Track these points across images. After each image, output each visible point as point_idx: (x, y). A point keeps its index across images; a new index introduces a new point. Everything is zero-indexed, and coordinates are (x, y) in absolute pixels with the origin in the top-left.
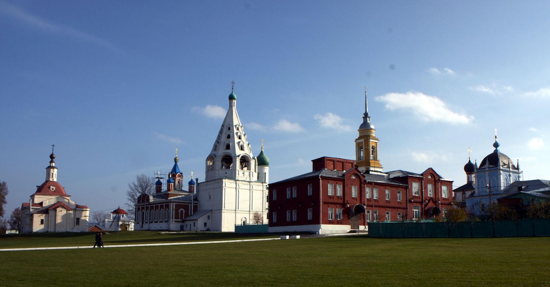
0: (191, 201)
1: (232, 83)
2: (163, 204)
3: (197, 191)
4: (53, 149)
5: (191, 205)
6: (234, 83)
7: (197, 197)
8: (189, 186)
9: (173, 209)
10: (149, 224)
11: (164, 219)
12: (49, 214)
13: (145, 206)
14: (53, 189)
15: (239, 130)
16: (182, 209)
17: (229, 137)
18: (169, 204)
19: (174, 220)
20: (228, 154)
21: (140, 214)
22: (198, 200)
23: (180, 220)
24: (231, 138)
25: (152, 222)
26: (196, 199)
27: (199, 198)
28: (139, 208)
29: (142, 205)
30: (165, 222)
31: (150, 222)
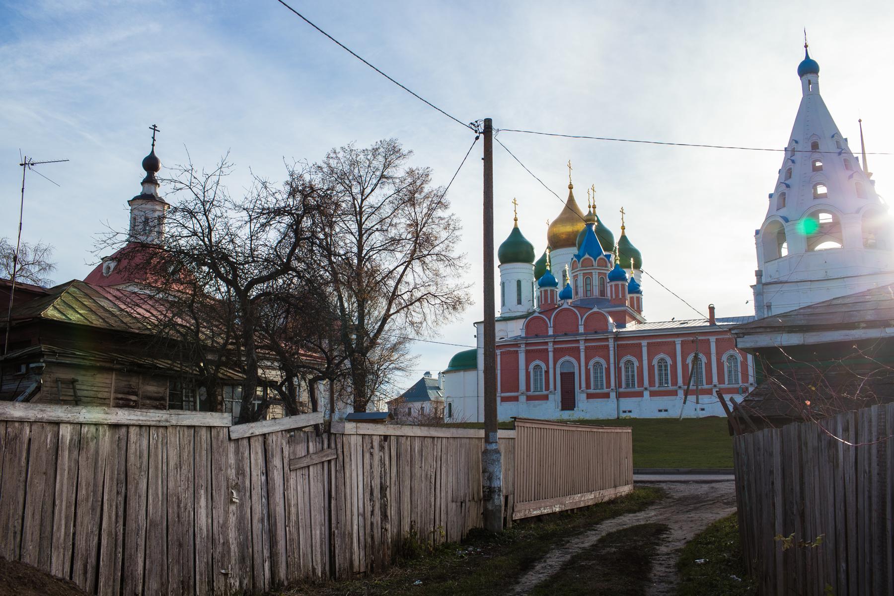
4: (154, 140)
11: (715, 380)
31: (619, 396)
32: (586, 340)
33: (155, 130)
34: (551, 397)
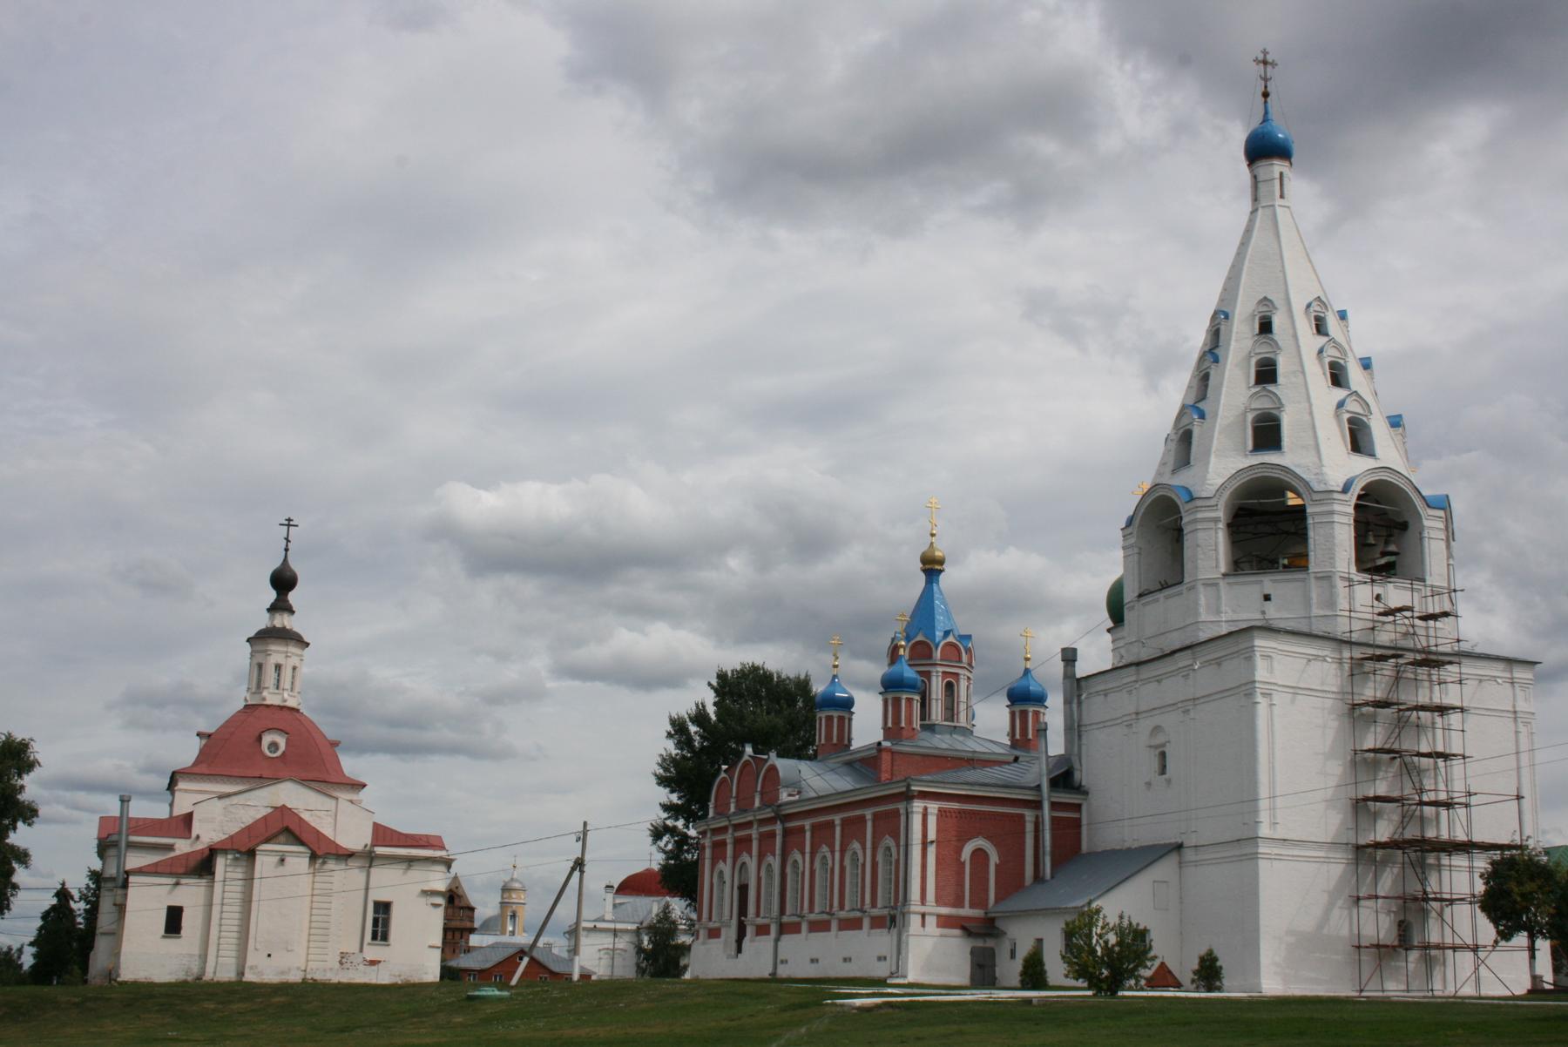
0: (1038, 788)
1: (1256, 61)
2: (858, 813)
3: (1074, 729)
4: (287, 540)
5: (1037, 817)
6: (1274, 64)
7: (1077, 766)
8: (1013, 714)
9: (925, 844)
10: (777, 940)
12: (213, 874)
13: (754, 833)
14: (274, 746)
15: (1327, 335)
16: (979, 842)
17: (1266, 374)
18: (901, 806)
19: (931, 907)
20: (1276, 474)
21: (727, 877)
22: (1079, 790)
23: (966, 911)
24: (1280, 379)
25: (794, 928)
26: (1064, 778)
27: (1083, 776)
28: (723, 844)
29: (737, 827)
30: (877, 923)
31: (784, 929)
32: (762, 822)
33: (289, 525)
34: (723, 931)
